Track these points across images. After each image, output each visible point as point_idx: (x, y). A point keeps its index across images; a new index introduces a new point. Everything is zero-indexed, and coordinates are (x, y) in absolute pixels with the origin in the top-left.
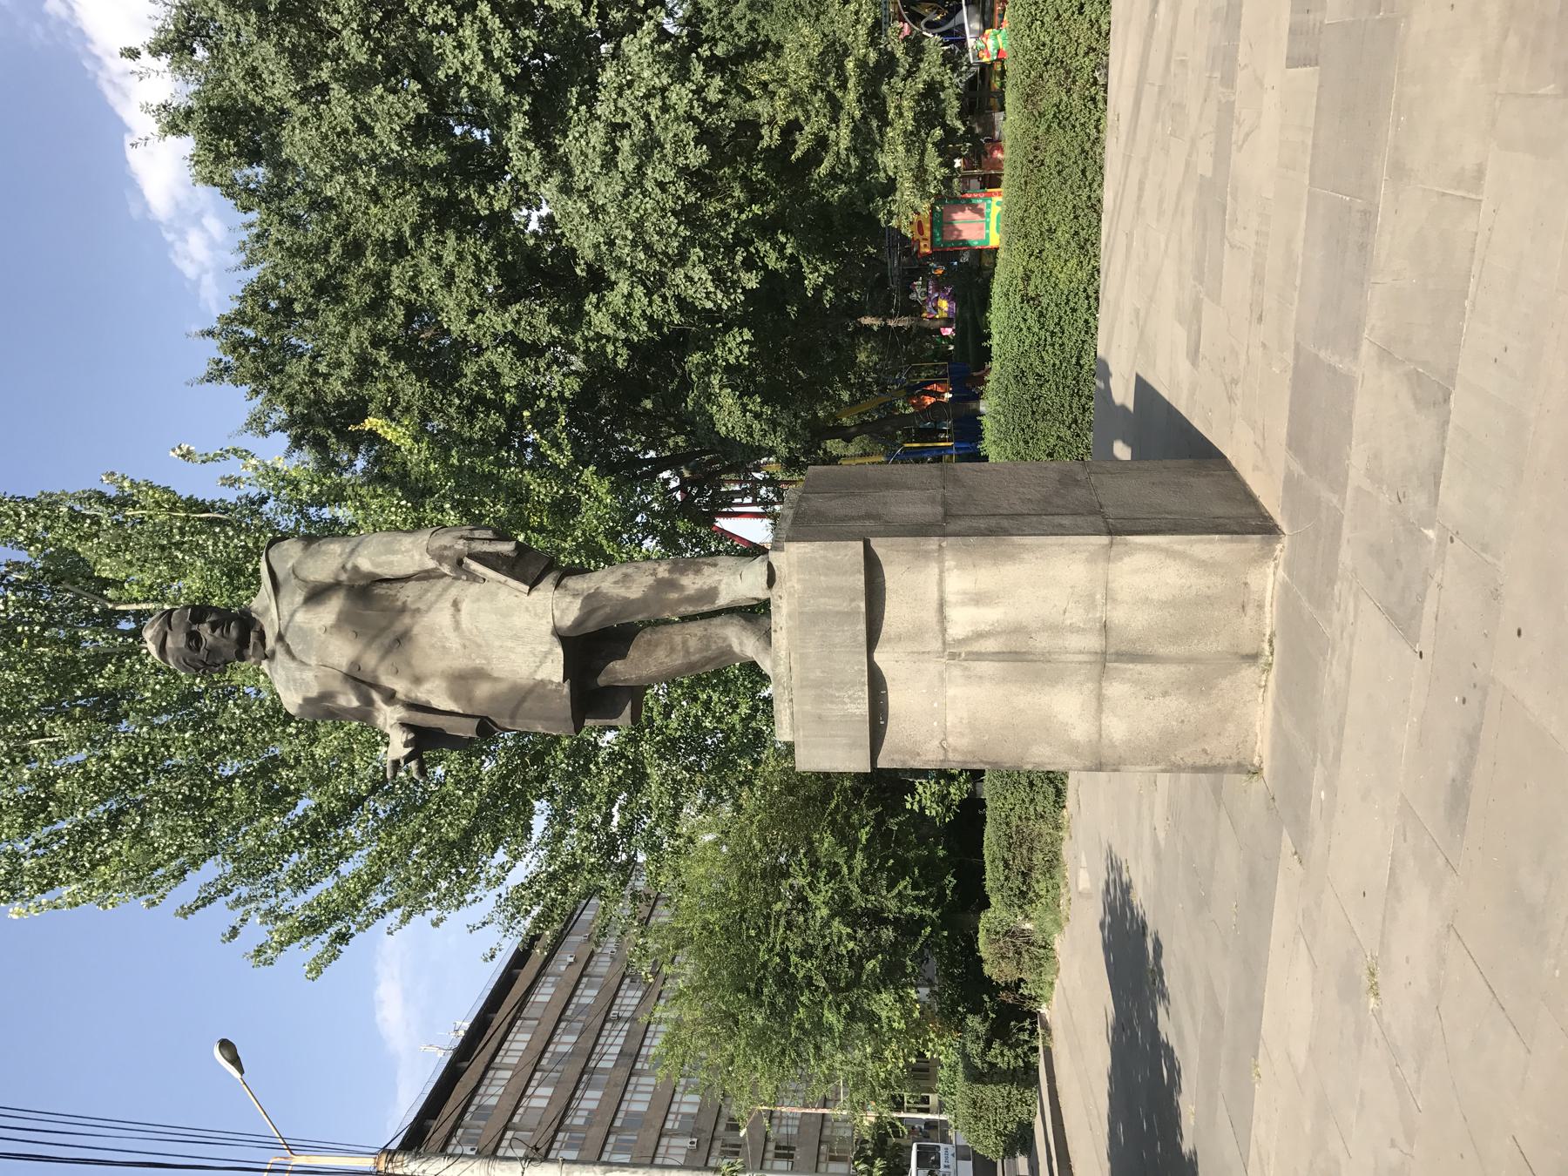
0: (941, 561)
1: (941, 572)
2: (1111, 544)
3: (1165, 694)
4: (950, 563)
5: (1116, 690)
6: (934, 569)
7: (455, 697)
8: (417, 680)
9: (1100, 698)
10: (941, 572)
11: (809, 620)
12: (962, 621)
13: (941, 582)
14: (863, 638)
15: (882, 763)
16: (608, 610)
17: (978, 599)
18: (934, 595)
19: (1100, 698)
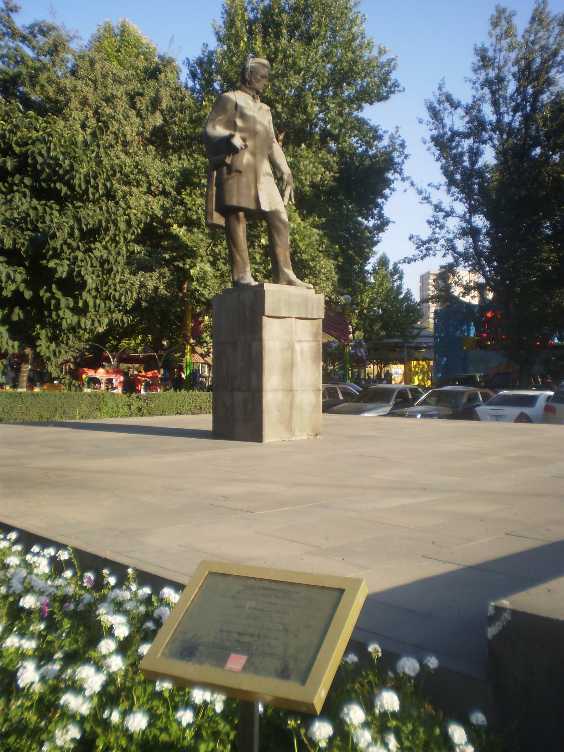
0: (313, 341)
1: (309, 341)
2: (320, 390)
3: (279, 411)
4: (312, 344)
5: (280, 395)
6: (310, 339)
7: (248, 165)
8: (254, 154)
9: (276, 391)
10: (309, 341)
11: (306, 300)
12: (298, 347)
13: (306, 341)
14: (301, 316)
15: (264, 318)
16: (284, 231)
17: (302, 352)
18: (303, 339)
19: (276, 391)
